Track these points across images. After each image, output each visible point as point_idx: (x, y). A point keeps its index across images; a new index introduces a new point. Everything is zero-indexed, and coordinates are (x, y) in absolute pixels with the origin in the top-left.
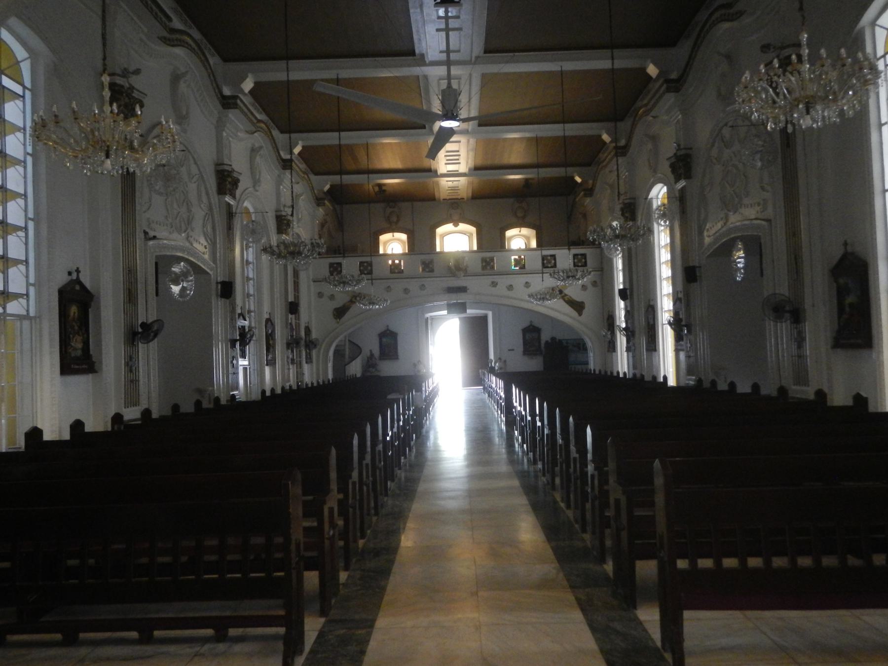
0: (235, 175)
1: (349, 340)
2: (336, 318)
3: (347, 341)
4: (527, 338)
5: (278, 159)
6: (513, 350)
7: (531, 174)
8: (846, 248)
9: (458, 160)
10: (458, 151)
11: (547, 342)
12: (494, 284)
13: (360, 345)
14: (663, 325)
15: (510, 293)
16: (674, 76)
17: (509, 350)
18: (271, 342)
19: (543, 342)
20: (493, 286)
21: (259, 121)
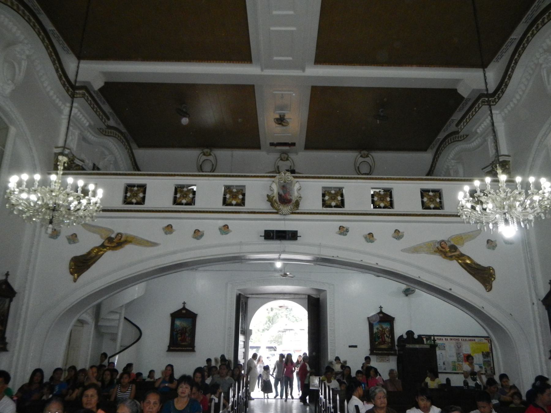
1: (125, 318)
2: (72, 273)
3: (122, 319)
4: (375, 330)
6: (356, 347)
11: (401, 337)
12: (343, 231)
17: (350, 347)
19: (396, 336)
20: (341, 234)
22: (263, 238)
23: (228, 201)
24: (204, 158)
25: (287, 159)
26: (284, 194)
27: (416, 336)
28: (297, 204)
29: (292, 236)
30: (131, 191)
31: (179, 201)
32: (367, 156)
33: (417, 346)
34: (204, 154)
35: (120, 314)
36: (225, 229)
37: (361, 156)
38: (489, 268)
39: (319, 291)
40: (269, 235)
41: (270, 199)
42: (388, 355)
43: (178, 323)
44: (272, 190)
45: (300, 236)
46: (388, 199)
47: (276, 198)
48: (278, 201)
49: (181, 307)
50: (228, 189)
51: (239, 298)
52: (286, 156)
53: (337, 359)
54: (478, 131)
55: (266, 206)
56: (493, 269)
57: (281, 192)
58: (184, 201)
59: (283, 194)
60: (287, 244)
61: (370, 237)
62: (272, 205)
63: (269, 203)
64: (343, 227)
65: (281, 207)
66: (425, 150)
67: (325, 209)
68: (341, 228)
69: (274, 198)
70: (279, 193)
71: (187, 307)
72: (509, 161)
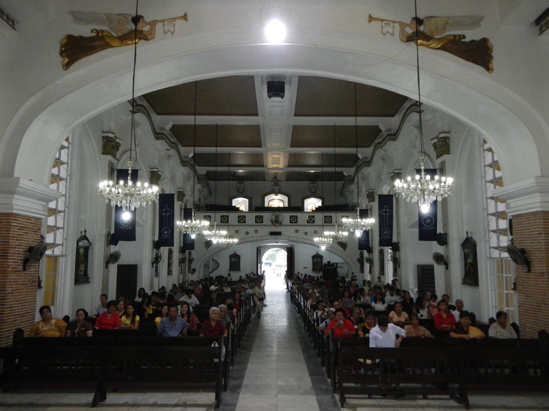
0: (160, 173)
1: (212, 259)
2: (206, 247)
4: (315, 261)
5: (180, 161)
6: (306, 268)
7: (319, 170)
8: (467, 235)
9: (279, 162)
10: (279, 158)
11: (325, 264)
12: (297, 231)
13: (218, 262)
14: (388, 260)
15: (305, 237)
16: (393, 132)
17: (304, 268)
18: (171, 262)
19: (323, 264)
21: (173, 143)
25: (278, 186)
27: (331, 263)
28: (281, 223)
29: (279, 234)
30: (223, 218)
31: (240, 221)
32: (314, 183)
33: (330, 268)
34: (240, 183)
36: (256, 231)
37: (312, 183)
38: (346, 243)
39: (292, 245)
40: (272, 234)
41: (272, 221)
42: (320, 271)
43: (232, 259)
47: (274, 221)
49: (233, 253)
50: (256, 217)
51: (258, 249)
53: (299, 273)
55: (270, 223)
57: (276, 219)
58: (242, 221)
60: (278, 237)
61: (306, 233)
62: (273, 223)
65: (276, 224)
68: (296, 230)
70: (275, 219)
71: (236, 253)
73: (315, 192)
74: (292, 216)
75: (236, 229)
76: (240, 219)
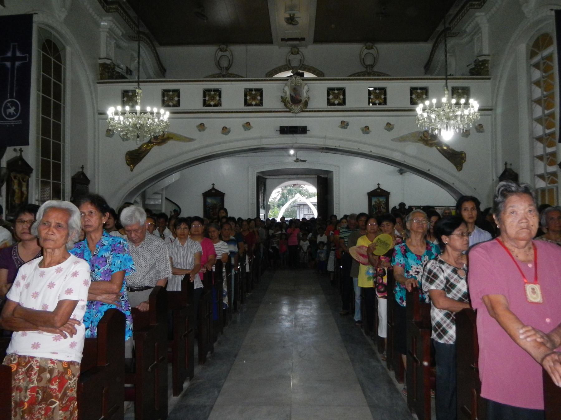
1: (166, 198)
2: (128, 165)
3: (164, 199)
4: (373, 203)
12: (344, 125)
19: (390, 209)
20: (342, 127)
22: (279, 132)
23: (249, 102)
24: (221, 53)
25: (298, 53)
26: (295, 95)
27: (407, 207)
28: (306, 104)
29: (303, 130)
30: (168, 96)
32: (372, 48)
34: (221, 50)
35: (162, 194)
36: (247, 126)
37: (366, 48)
38: (461, 153)
41: (283, 100)
43: (209, 200)
44: (285, 93)
45: (309, 130)
46: (383, 97)
47: (289, 99)
48: (290, 101)
49: (211, 187)
51: (258, 178)
52: (297, 50)
54: (467, 30)
55: (280, 106)
56: (465, 154)
57: (293, 94)
58: (212, 103)
59: (294, 95)
61: (366, 130)
62: (285, 105)
63: (283, 104)
64: (344, 122)
65: (293, 107)
66: (426, 40)
67: (329, 107)
68: (342, 122)
69: (287, 99)
70: (291, 95)
72: (489, 60)
73: (372, 66)
74: (333, 89)
75: (199, 121)
76: (207, 98)
